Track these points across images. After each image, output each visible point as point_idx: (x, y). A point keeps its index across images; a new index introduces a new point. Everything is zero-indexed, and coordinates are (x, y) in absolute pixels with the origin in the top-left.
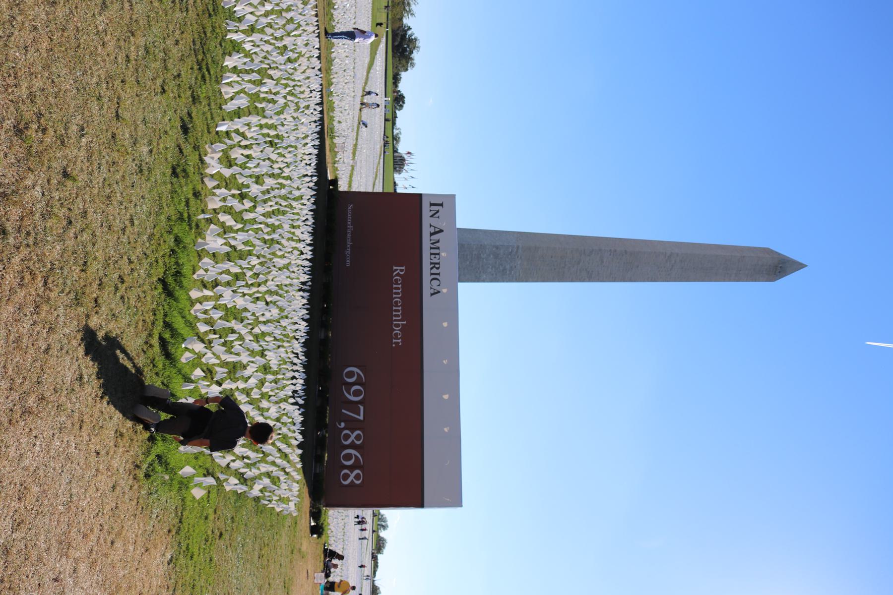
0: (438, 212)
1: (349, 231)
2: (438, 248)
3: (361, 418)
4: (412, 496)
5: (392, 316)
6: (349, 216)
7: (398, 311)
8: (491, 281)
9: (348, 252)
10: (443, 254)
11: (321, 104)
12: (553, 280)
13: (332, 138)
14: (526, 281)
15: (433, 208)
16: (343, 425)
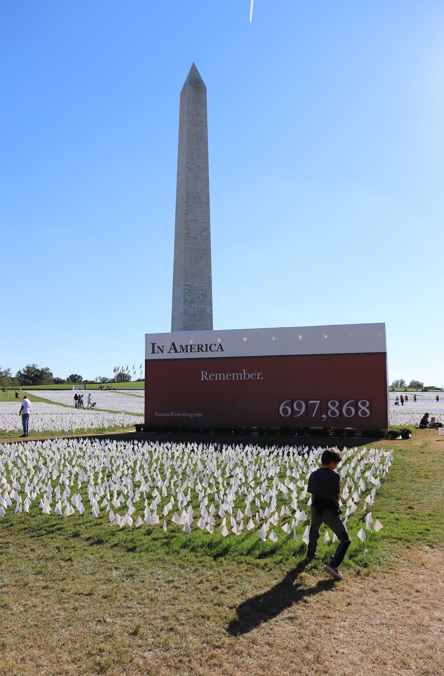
0: (159, 347)
1: (175, 415)
2: (187, 346)
3: (318, 402)
5: (239, 380)
6: (164, 415)
7: (235, 376)
8: (211, 305)
9: (191, 415)
10: (191, 342)
11: (78, 439)
12: (210, 257)
13: (104, 429)
14: (211, 278)
15: (156, 350)
16: (324, 416)
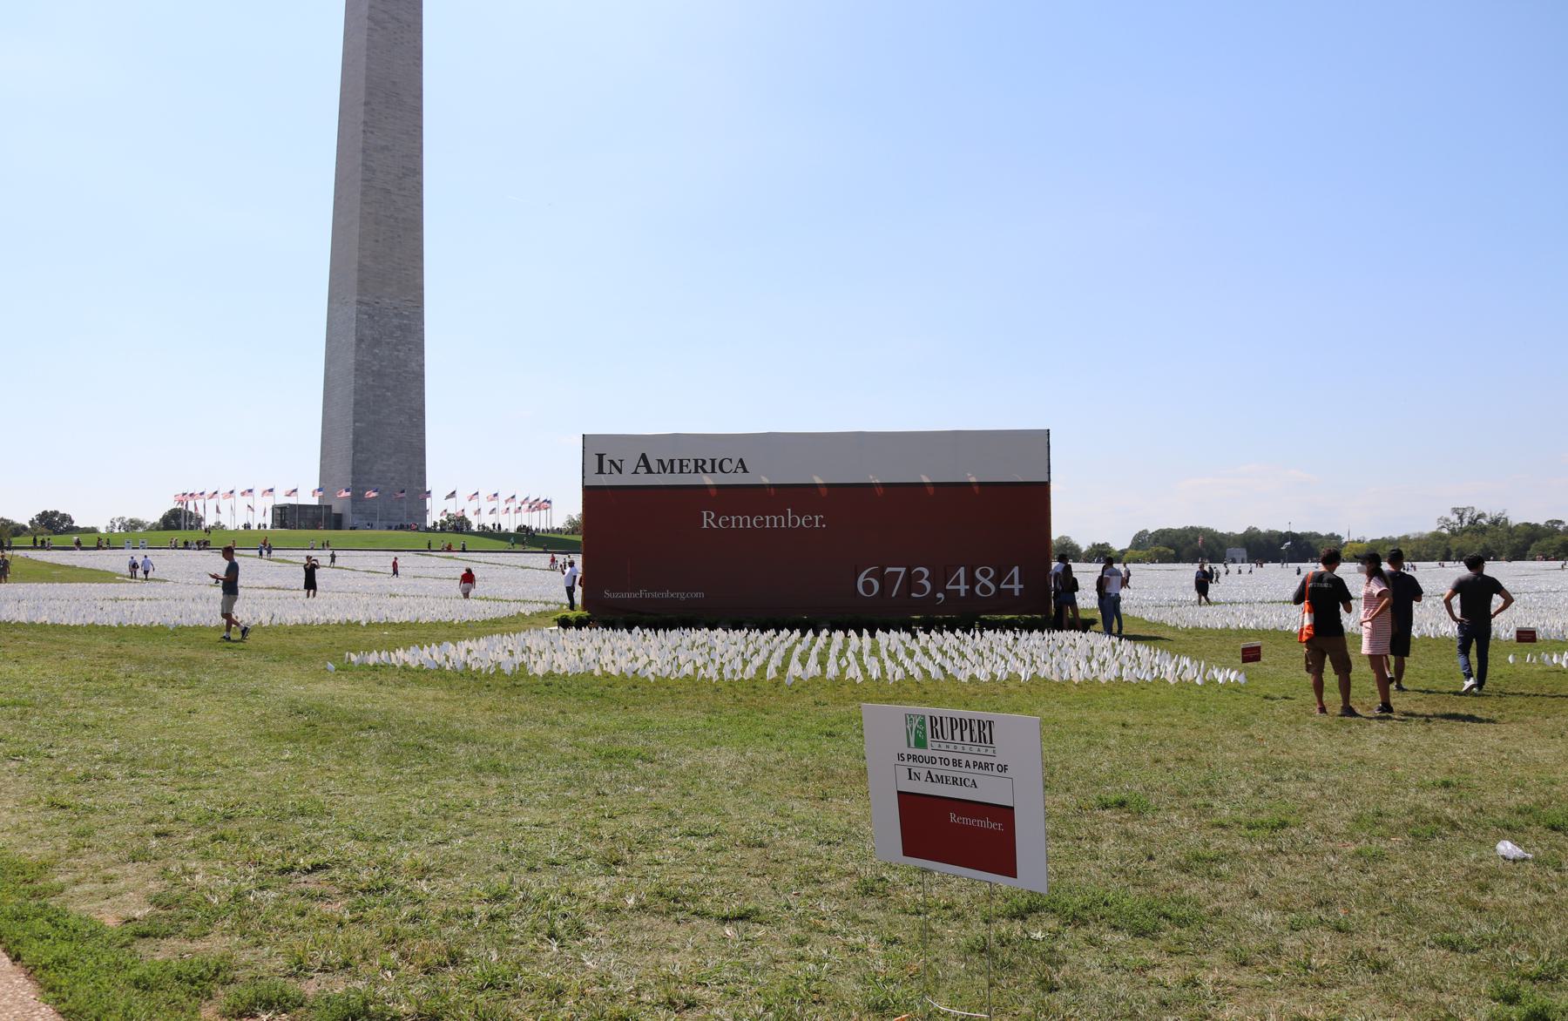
0: (612, 462)
1: (648, 595)
2: (672, 461)
4: (1037, 494)
6: (623, 596)
7: (772, 521)
8: (422, 352)
9: (682, 596)
16: (940, 595)
